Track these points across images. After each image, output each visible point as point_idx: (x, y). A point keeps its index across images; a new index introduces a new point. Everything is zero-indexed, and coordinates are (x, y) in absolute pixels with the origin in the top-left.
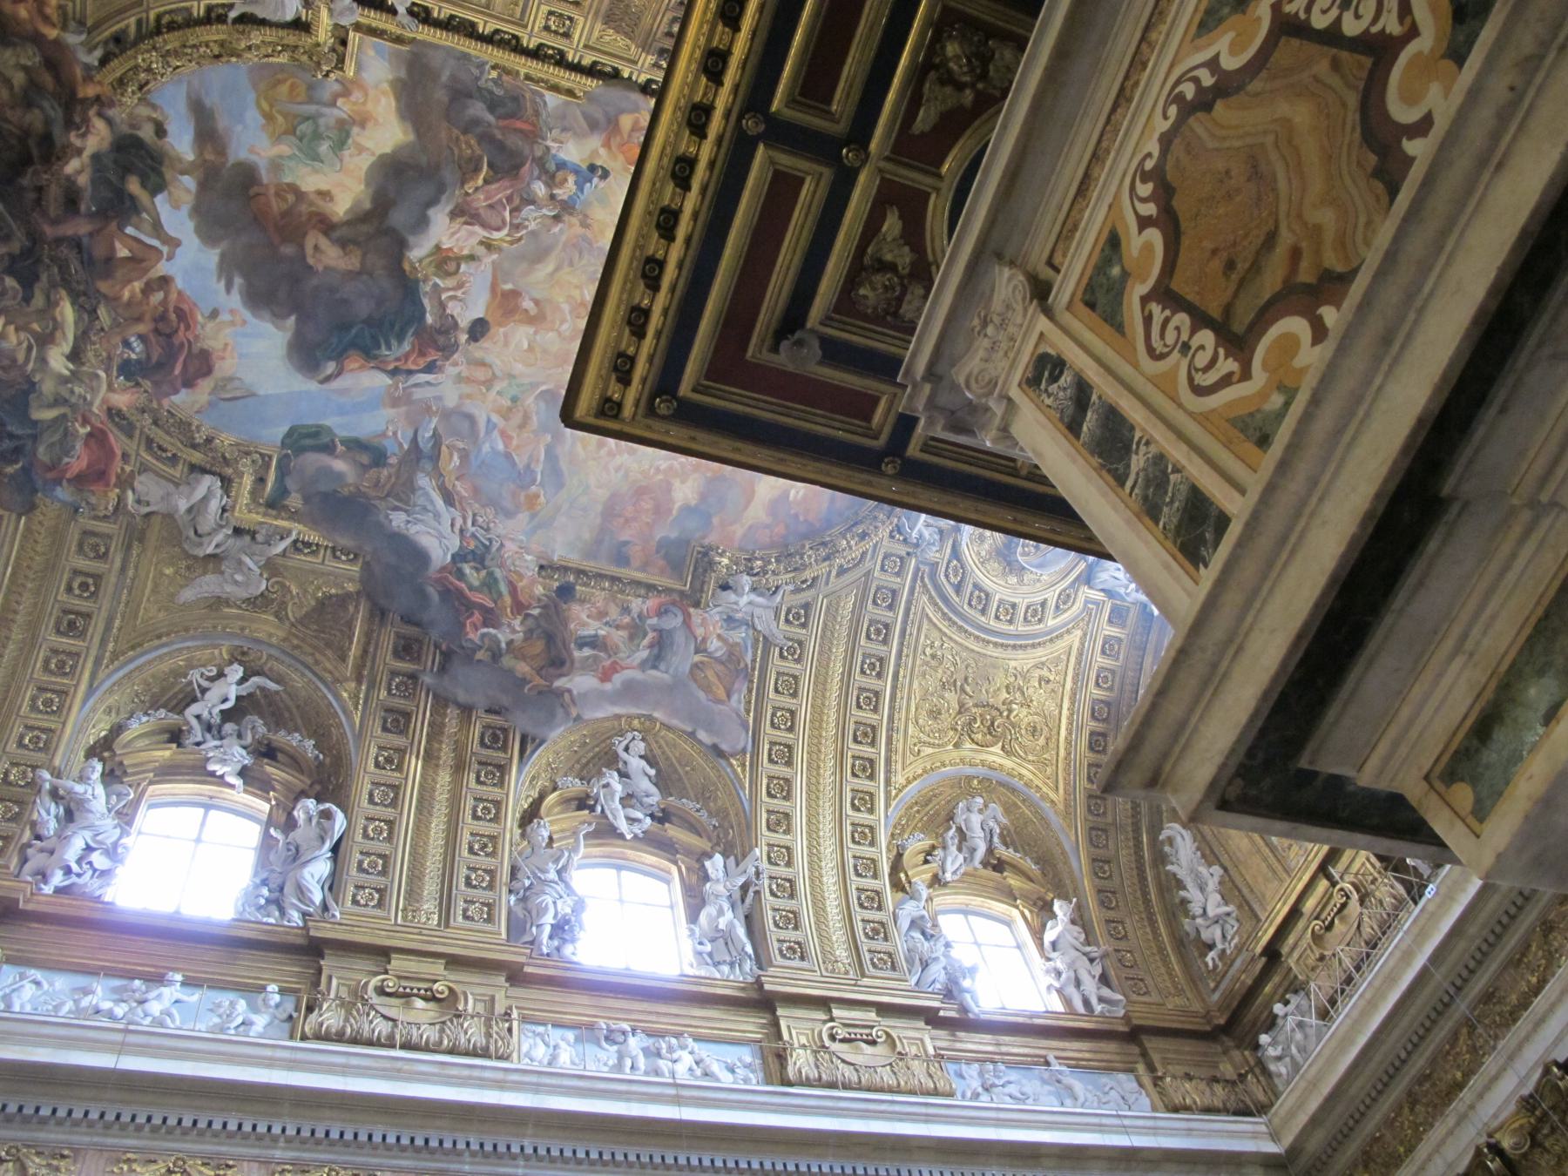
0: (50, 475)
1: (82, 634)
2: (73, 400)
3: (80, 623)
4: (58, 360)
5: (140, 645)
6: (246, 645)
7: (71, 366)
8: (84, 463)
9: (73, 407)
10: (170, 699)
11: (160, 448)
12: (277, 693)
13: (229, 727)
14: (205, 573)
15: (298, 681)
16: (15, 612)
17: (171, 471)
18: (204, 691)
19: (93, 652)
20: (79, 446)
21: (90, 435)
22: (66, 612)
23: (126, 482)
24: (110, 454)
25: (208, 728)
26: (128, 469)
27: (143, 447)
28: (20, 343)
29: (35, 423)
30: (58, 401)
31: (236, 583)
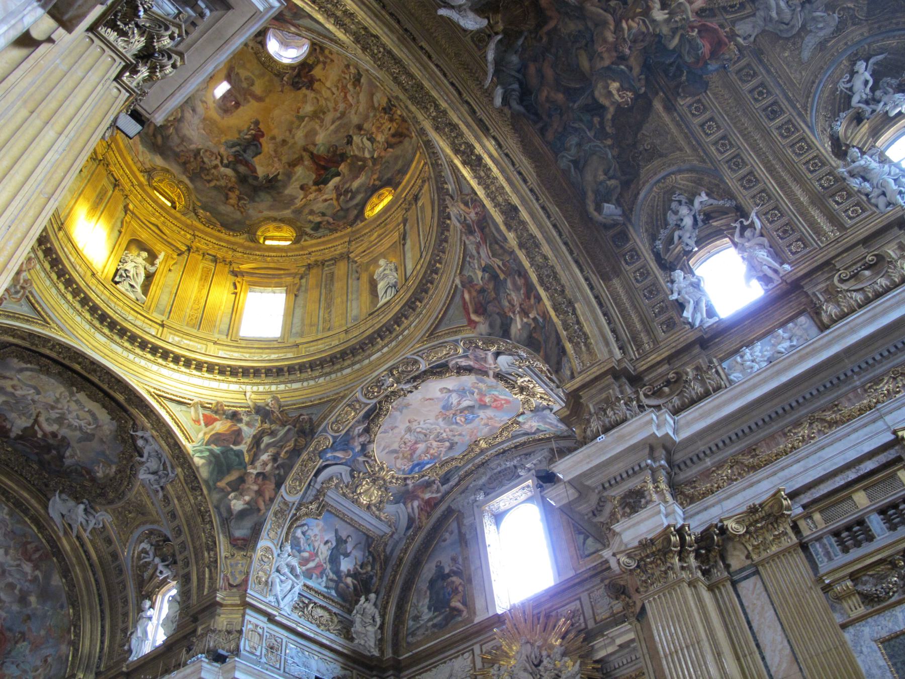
0: (700, 64)
1: (782, 112)
2: (680, 25)
3: (775, 108)
4: (659, 15)
5: (810, 92)
6: (854, 50)
7: (666, 11)
8: (708, 46)
9: (682, 28)
10: (839, 107)
11: (731, 7)
12: (885, 58)
13: (878, 93)
14: (803, 39)
15: (893, 43)
16: (746, 129)
17: (746, 12)
18: (851, 89)
19: (794, 114)
20: (699, 41)
21: (699, 32)
22: (765, 110)
23: (732, 36)
24: (715, 29)
25: (867, 102)
26: (727, 29)
27: (725, 15)
28: (638, 24)
29: (674, 48)
30: (674, 31)
31: (821, 29)
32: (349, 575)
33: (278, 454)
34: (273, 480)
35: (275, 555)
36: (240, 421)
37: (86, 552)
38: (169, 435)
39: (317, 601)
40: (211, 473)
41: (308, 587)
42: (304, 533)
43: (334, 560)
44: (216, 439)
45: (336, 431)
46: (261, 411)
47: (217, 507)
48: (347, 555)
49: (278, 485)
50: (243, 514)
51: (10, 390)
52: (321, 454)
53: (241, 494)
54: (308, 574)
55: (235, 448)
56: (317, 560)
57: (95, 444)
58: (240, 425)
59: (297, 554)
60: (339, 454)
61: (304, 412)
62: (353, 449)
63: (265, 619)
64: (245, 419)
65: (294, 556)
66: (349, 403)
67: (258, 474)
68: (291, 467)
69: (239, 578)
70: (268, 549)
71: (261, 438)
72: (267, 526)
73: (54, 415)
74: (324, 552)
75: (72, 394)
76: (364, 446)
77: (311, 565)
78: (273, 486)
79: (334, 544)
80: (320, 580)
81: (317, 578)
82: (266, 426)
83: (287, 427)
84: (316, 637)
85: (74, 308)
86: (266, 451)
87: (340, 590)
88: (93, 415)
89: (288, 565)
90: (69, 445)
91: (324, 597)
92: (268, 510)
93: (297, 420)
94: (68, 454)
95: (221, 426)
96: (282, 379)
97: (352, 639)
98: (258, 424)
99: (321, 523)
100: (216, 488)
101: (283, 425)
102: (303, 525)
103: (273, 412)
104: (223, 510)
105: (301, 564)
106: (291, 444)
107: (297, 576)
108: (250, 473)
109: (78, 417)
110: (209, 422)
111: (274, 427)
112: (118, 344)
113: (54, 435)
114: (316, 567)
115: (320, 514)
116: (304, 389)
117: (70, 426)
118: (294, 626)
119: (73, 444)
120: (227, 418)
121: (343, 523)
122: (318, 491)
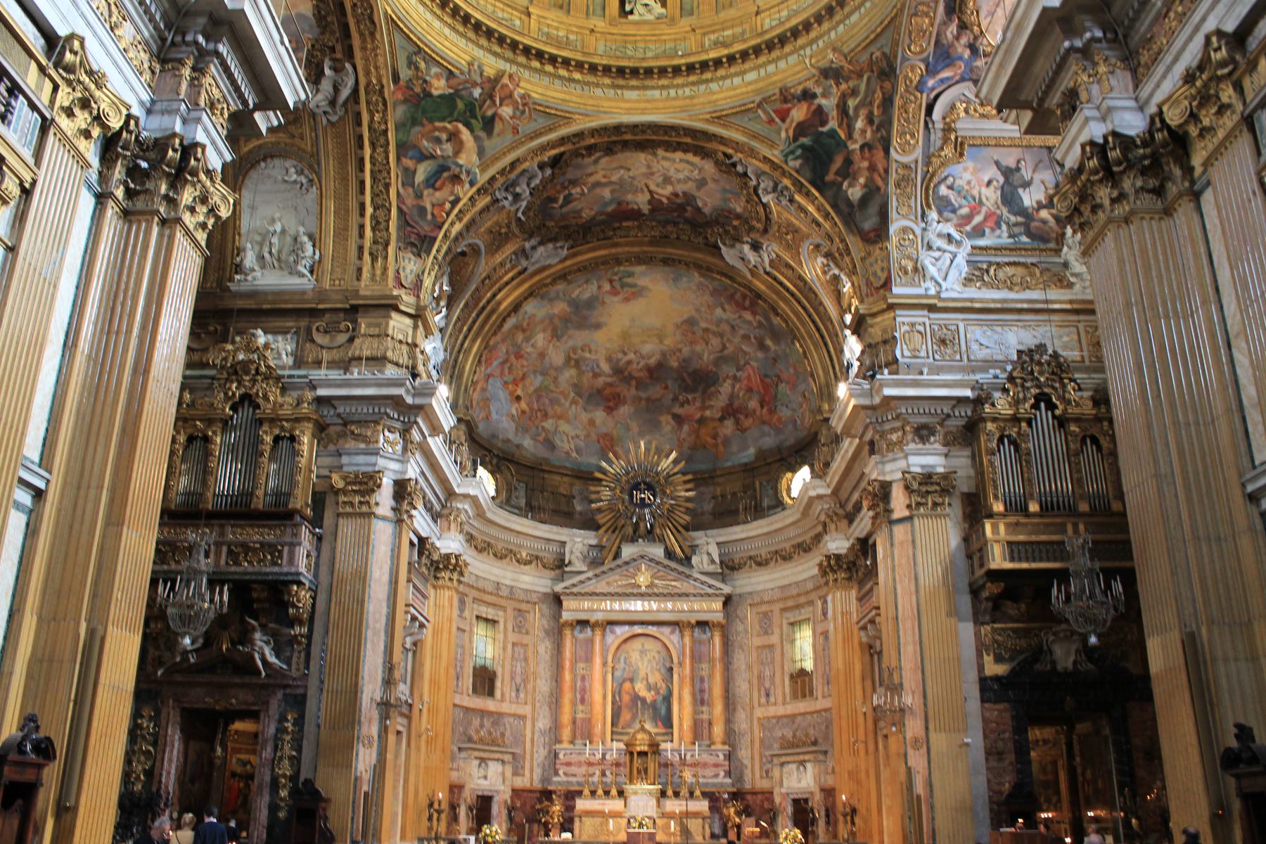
32: (1040, 206)
33: (871, 113)
34: (880, 148)
35: (918, 231)
36: (814, 96)
37: (781, 284)
38: (752, 153)
39: (998, 259)
40: (814, 170)
41: (981, 248)
42: (951, 188)
43: (1009, 198)
44: (801, 129)
45: (922, 52)
46: (830, 73)
47: (834, 206)
48: (1026, 185)
49: (887, 152)
50: (864, 201)
51: (604, 180)
52: (920, 87)
53: (855, 178)
54: (979, 232)
55: (825, 129)
56: (984, 210)
57: (711, 185)
58: (817, 101)
59: (951, 215)
60: (946, 74)
61: (872, 49)
62: (960, 58)
63: (926, 313)
64: (818, 91)
65: (947, 220)
66: (913, 11)
67: (862, 147)
68: (890, 123)
69: (883, 276)
70: (905, 230)
71: (845, 103)
72: (893, 203)
73: (660, 180)
74: (991, 196)
75: (655, 155)
76: (973, 48)
77: (978, 219)
78: (881, 154)
79: (1002, 180)
80: (998, 232)
81: (993, 230)
82: (844, 86)
83: (865, 78)
84: (1006, 306)
85: (587, 84)
86: (857, 116)
87: (1033, 230)
88: (688, 162)
89: (940, 235)
90: (694, 198)
91: (1011, 250)
92: (887, 184)
93: (871, 63)
94: (700, 204)
95: (799, 113)
96: (837, 17)
97: (1070, 285)
98: (834, 90)
99: (970, 164)
100: (825, 184)
101: (860, 76)
102: (946, 178)
103: (842, 67)
104: (843, 206)
105: (959, 227)
106: (878, 95)
107: (959, 244)
108: (853, 150)
109: (678, 171)
110: (784, 115)
111: (851, 84)
112: (653, 88)
113: (676, 195)
114: (986, 219)
115: (961, 155)
116: (861, 19)
117: (679, 181)
118: (968, 304)
119: (697, 194)
120: (799, 101)
121: (1001, 150)
122: (944, 130)
